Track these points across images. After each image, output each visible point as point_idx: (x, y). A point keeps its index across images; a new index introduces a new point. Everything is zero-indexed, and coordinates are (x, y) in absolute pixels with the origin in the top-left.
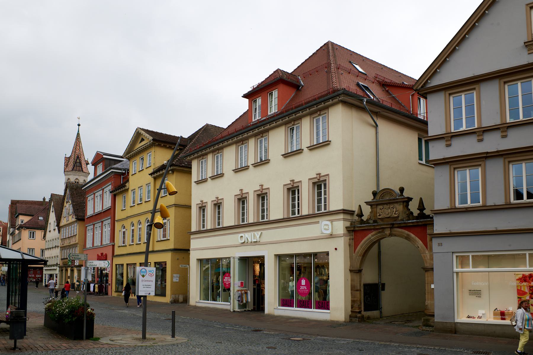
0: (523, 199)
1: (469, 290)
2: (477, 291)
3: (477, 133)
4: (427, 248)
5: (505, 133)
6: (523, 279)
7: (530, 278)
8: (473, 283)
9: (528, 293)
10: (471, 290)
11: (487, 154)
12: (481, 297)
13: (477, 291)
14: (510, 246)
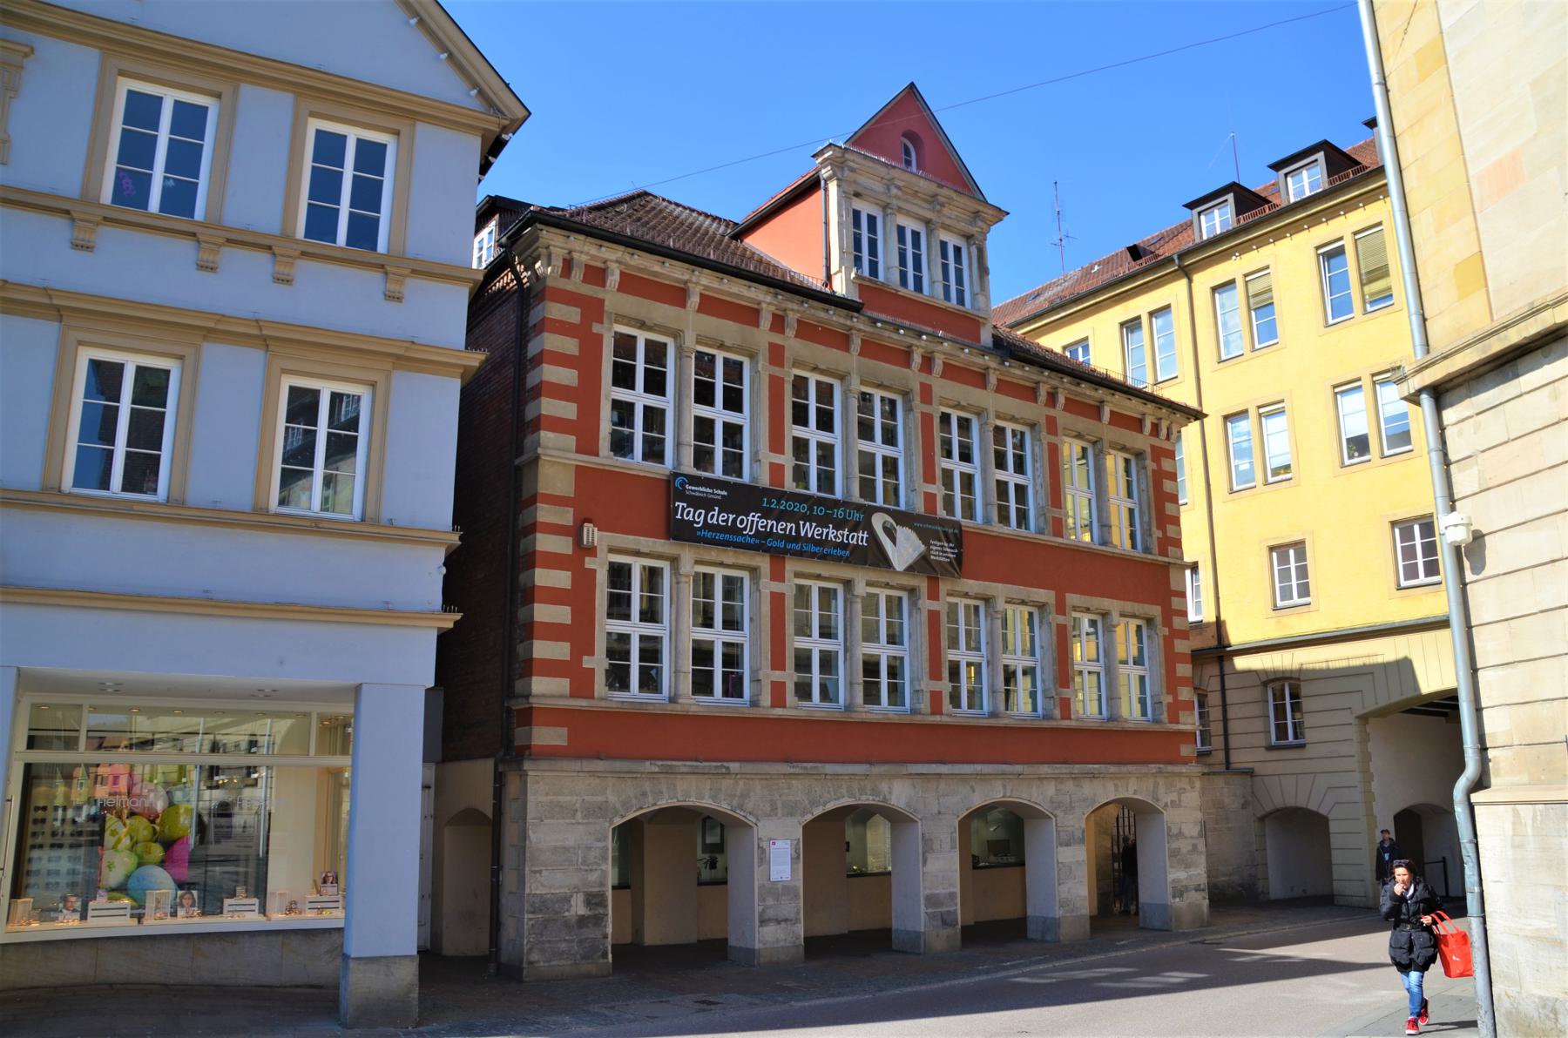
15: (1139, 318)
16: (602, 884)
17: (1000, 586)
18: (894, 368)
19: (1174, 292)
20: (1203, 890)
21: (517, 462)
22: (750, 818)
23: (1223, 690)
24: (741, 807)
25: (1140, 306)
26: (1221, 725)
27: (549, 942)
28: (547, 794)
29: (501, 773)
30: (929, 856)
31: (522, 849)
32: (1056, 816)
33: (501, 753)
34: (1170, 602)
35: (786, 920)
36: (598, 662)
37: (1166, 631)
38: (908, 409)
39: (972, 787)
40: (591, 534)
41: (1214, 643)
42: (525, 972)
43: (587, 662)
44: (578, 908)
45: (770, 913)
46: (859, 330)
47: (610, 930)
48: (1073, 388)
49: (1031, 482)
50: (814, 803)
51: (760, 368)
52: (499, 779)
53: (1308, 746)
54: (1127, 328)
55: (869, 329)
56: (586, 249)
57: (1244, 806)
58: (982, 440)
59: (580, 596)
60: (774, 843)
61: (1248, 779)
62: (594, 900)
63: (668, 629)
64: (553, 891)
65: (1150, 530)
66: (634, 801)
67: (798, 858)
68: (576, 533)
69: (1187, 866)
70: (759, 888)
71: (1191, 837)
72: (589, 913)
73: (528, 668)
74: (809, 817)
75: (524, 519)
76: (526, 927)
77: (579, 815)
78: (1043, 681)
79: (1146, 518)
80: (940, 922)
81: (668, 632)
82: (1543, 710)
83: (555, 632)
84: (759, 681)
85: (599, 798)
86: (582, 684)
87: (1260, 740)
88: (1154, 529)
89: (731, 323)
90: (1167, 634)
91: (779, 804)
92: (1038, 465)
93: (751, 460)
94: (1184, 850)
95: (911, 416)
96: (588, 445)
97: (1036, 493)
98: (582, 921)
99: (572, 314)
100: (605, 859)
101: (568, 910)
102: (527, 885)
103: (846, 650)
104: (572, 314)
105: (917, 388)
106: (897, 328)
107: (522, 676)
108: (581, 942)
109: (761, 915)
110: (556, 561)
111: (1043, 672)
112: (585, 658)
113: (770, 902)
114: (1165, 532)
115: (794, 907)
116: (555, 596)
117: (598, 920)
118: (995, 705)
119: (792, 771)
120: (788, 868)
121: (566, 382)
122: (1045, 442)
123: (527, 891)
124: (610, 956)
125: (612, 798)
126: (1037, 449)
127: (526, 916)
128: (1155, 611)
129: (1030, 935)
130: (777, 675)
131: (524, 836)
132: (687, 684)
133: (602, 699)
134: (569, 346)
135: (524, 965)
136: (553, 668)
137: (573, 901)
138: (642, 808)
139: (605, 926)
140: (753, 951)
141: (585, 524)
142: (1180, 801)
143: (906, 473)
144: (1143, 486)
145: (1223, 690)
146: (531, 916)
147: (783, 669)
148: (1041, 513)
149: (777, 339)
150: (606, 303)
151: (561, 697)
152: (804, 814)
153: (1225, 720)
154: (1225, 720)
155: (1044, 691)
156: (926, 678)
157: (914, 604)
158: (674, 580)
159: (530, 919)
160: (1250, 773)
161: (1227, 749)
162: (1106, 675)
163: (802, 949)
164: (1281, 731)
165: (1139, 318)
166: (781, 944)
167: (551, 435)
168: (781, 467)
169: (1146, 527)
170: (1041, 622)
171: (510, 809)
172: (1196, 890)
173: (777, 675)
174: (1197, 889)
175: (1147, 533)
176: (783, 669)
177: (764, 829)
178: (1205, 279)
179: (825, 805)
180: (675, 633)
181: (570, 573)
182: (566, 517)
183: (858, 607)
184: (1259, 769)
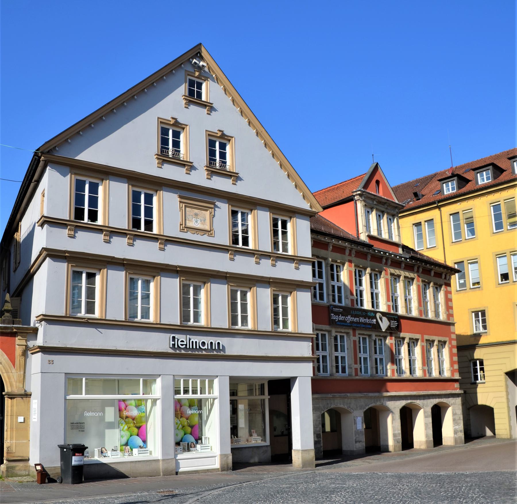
1: (71, 423)
2: (81, 423)
4: (14, 365)
8: (86, 413)
10: (73, 423)
12: (84, 431)
13: (81, 423)
14: (127, 369)
16: (320, 431)
17: (407, 334)
18: (377, 263)
19: (434, 214)
20: (462, 432)
22: (352, 410)
24: (349, 407)
25: (422, 217)
30: (394, 421)
35: (361, 441)
45: (357, 439)
47: (322, 445)
50: (366, 405)
53: (486, 383)
74: (365, 410)
80: (396, 442)
81: (328, 354)
84: (351, 368)
85: (318, 406)
89: (339, 254)
90: (450, 347)
91: (358, 406)
103: (370, 357)
109: (355, 439)
119: (362, 395)
120: (361, 425)
125: (321, 405)
128: (447, 339)
138: (327, 408)
140: (354, 451)
147: (357, 364)
152: (364, 409)
158: (329, 338)
166: (360, 449)
176: (357, 364)
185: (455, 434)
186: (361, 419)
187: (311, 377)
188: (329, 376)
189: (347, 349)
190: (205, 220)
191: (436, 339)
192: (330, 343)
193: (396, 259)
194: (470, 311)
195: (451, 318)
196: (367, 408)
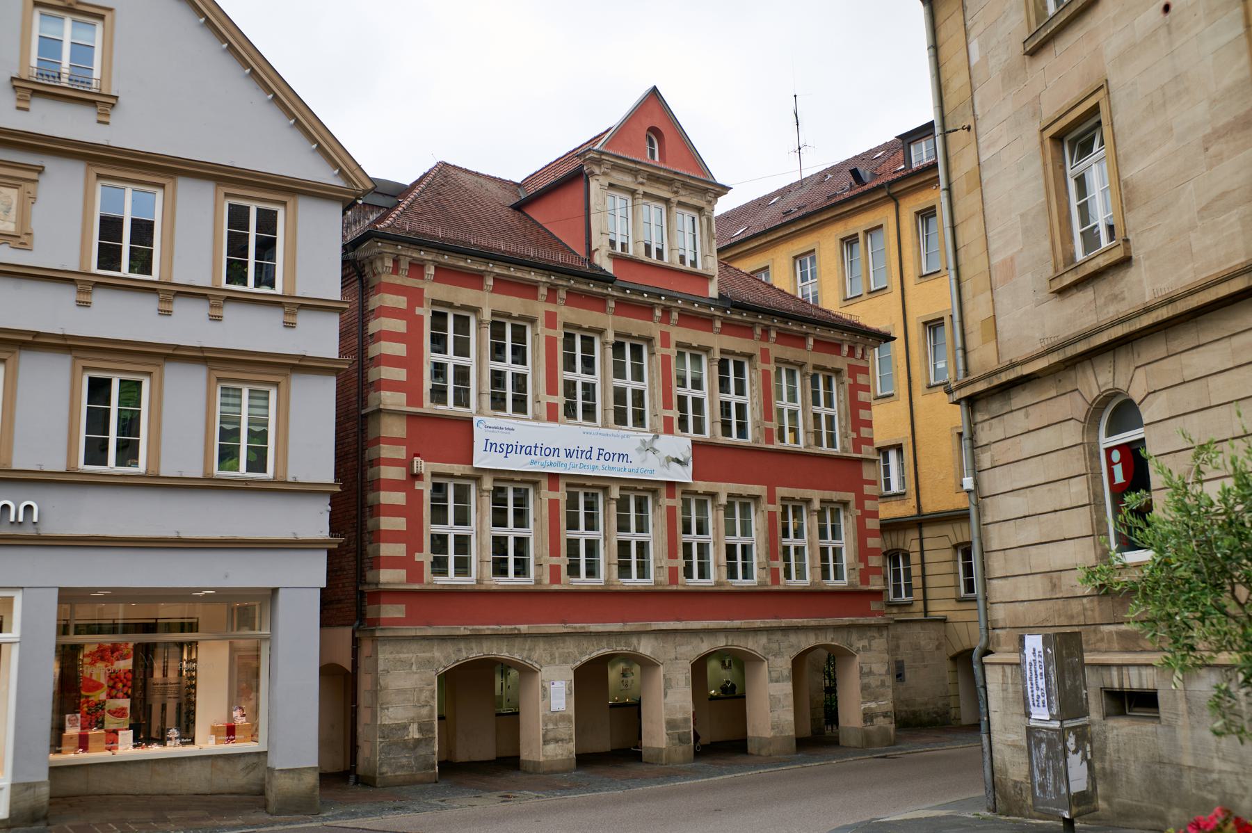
0: (106, 464)
3: (209, 300)
5: (85, 296)
6: (99, 654)
7: (113, 652)
9: (106, 686)
11: (34, 337)
15: (857, 235)
16: (431, 716)
17: (723, 484)
19: (884, 215)
20: (890, 716)
21: (363, 412)
23: (922, 551)
25: (859, 224)
26: (920, 580)
27: (394, 758)
28: (391, 653)
29: (357, 638)
31: (375, 692)
32: (768, 660)
33: (357, 623)
34: (862, 489)
35: (562, 740)
36: (426, 556)
37: (859, 512)
38: (652, 354)
39: (702, 638)
40: (421, 465)
41: (915, 512)
42: (378, 780)
43: (418, 557)
44: (414, 733)
45: (551, 735)
46: (613, 296)
47: (436, 749)
48: (782, 325)
49: (749, 401)
50: (582, 653)
51: (539, 331)
52: (356, 642)
54: (847, 243)
55: (621, 295)
56: (409, 254)
57: (938, 648)
58: (709, 371)
59: (411, 510)
60: (553, 684)
61: (942, 626)
62: (424, 728)
63: (475, 529)
64: (396, 722)
65: (847, 433)
66: (453, 655)
67: (571, 693)
68: (408, 464)
69: (876, 699)
70: (543, 716)
71: (880, 675)
72: (421, 737)
73: (378, 563)
74: (578, 664)
75: (370, 454)
76: (378, 748)
77: (414, 668)
78: (758, 555)
79: (843, 423)
80: (677, 741)
81: (474, 532)
82: (1019, 607)
83: (395, 536)
85: (428, 655)
86: (415, 571)
87: (951, 593)
88: (850, 432)
89: (517, 298)
91: (557, 655)
92: (754, 388)
93: (533, 401)
94: (873, 685)
95: (654, 358)
96: (415, 399)
97: (753, 409)
98: (417, 742)
99: (400, 302)
100: (433, 698)
101: (408, 736)
102: (379, 718)
104: (400, 302)
105: (658, 336)
106: (642, 293)
107: (372, 568)
108: (416, 758)
110: (394, 486)
111: (758, 549)
112: (417, 554)
113: (551, 726)
114: (859, 434)
115: (568, 730)
116: (395, 511)
117: (427, 741)
118: (719, 576)
120: (564, 701)
121: (398, 354)
122: (760, 369)
123: (379, 723)
124: (437, 767)
126: (753, 375)
127: (378, 740)
128: (850, 496)
129: (749, 749)
130: (555, 560)
131: (376, 682)
132: (489, 568)
133: (429, 584)
134: (400, 326)
135: (377, 775)
136: (395, 563)
137: (411, 729)
139: (433, 747)
140: (539, 763)
141: (415, 458)
142: (870, 645)
143: (650, 401)
144: (842, 398)
145: (922, 551)
146: (381, 740)
147: (559, 555)
148: (757, 426)
149: (551, 308)
150: (425, 291)
151: (401, 583)
152: (574, 661)
153: (924, 576)
154: (924, 576)
155: (759, 563)
156: (665, 558)
157: (656, 502)
158: (479, 495)
159: (381, 743)
160: (944, 621)
161: (925, 600)
162: (809, 548)
163: (574, 762)
164: (970, 587)
165: (857, 235)
166: (559, 757)
167: (388, 393)
168: (555, 405)
169: (843, 430)
170: (756, 510)
171: (364, 664)
172: (884, 717)
173: (555, 560)
174: (885, 715)
175: (844, 436)
176: (559, 555)
177: (545, 674)
178: (911, 205)
179: (590, 655)
180: (479, 534)
181: (404, 494)
182: (401, 453)
183: (614, 507)
184: (951, 616)
185: (865, 721)
186: (564, 686)
187: (322, 589)
188: (474, 583)
189: (535, 520)
190: (7, 211)
191: (816, 496)
192: (479, 507)
193: (693, 309)
194: (955, 431)
195: (864, 447)
196: (585, 658)
